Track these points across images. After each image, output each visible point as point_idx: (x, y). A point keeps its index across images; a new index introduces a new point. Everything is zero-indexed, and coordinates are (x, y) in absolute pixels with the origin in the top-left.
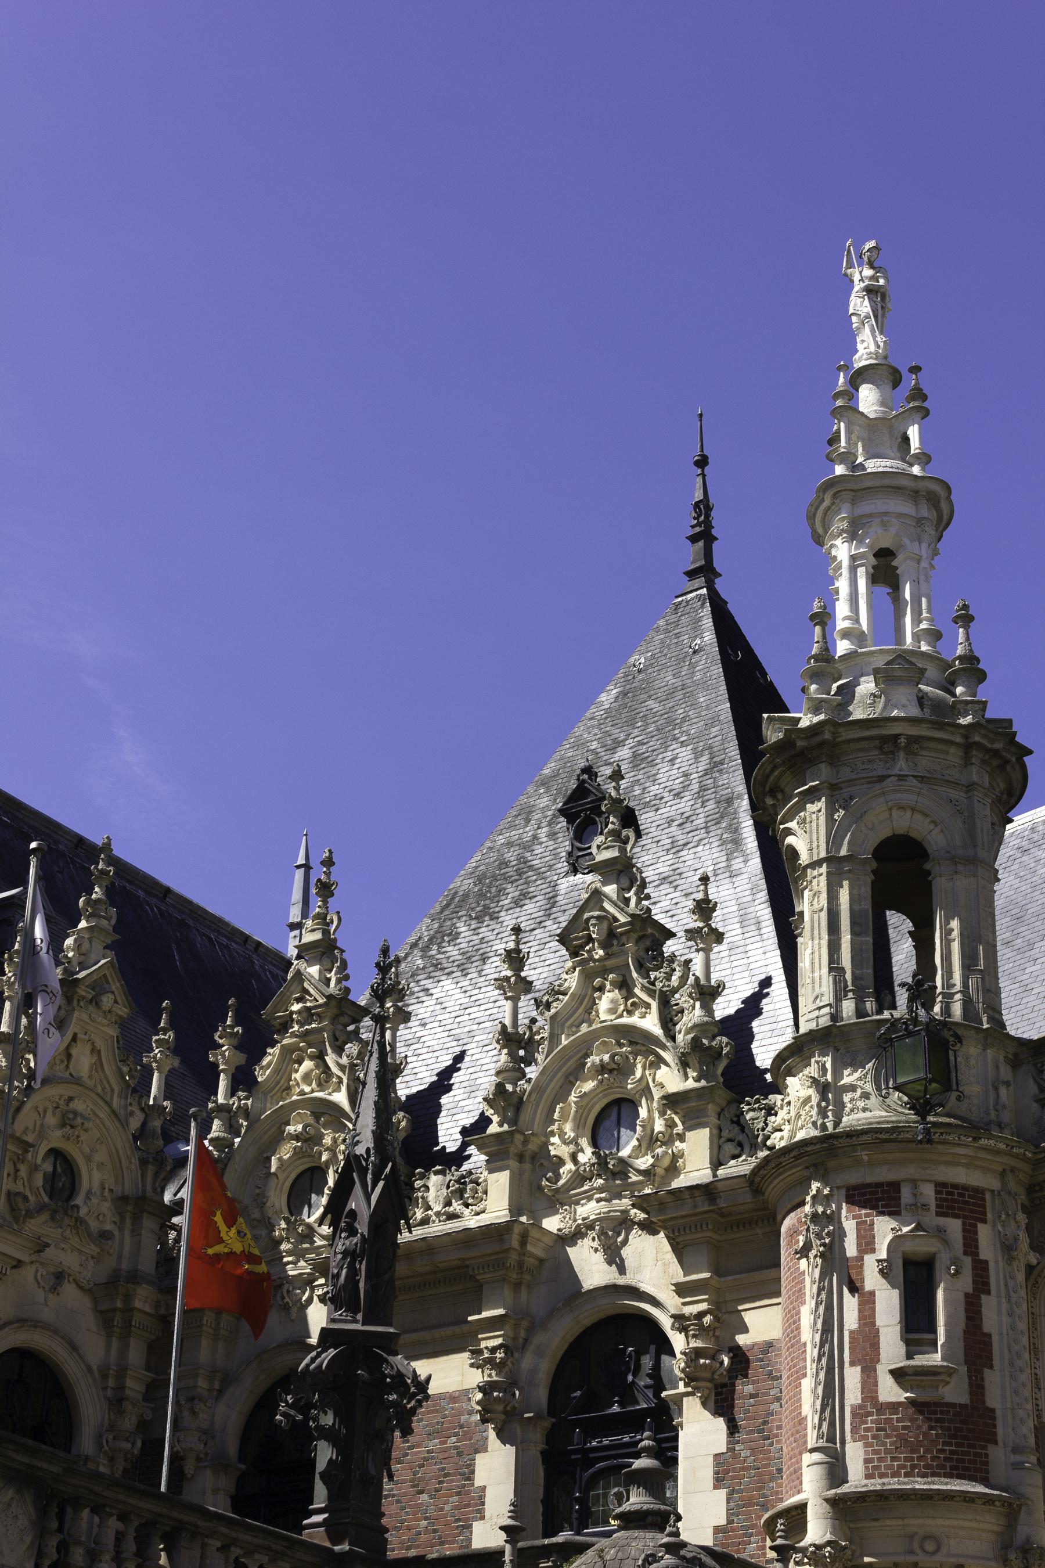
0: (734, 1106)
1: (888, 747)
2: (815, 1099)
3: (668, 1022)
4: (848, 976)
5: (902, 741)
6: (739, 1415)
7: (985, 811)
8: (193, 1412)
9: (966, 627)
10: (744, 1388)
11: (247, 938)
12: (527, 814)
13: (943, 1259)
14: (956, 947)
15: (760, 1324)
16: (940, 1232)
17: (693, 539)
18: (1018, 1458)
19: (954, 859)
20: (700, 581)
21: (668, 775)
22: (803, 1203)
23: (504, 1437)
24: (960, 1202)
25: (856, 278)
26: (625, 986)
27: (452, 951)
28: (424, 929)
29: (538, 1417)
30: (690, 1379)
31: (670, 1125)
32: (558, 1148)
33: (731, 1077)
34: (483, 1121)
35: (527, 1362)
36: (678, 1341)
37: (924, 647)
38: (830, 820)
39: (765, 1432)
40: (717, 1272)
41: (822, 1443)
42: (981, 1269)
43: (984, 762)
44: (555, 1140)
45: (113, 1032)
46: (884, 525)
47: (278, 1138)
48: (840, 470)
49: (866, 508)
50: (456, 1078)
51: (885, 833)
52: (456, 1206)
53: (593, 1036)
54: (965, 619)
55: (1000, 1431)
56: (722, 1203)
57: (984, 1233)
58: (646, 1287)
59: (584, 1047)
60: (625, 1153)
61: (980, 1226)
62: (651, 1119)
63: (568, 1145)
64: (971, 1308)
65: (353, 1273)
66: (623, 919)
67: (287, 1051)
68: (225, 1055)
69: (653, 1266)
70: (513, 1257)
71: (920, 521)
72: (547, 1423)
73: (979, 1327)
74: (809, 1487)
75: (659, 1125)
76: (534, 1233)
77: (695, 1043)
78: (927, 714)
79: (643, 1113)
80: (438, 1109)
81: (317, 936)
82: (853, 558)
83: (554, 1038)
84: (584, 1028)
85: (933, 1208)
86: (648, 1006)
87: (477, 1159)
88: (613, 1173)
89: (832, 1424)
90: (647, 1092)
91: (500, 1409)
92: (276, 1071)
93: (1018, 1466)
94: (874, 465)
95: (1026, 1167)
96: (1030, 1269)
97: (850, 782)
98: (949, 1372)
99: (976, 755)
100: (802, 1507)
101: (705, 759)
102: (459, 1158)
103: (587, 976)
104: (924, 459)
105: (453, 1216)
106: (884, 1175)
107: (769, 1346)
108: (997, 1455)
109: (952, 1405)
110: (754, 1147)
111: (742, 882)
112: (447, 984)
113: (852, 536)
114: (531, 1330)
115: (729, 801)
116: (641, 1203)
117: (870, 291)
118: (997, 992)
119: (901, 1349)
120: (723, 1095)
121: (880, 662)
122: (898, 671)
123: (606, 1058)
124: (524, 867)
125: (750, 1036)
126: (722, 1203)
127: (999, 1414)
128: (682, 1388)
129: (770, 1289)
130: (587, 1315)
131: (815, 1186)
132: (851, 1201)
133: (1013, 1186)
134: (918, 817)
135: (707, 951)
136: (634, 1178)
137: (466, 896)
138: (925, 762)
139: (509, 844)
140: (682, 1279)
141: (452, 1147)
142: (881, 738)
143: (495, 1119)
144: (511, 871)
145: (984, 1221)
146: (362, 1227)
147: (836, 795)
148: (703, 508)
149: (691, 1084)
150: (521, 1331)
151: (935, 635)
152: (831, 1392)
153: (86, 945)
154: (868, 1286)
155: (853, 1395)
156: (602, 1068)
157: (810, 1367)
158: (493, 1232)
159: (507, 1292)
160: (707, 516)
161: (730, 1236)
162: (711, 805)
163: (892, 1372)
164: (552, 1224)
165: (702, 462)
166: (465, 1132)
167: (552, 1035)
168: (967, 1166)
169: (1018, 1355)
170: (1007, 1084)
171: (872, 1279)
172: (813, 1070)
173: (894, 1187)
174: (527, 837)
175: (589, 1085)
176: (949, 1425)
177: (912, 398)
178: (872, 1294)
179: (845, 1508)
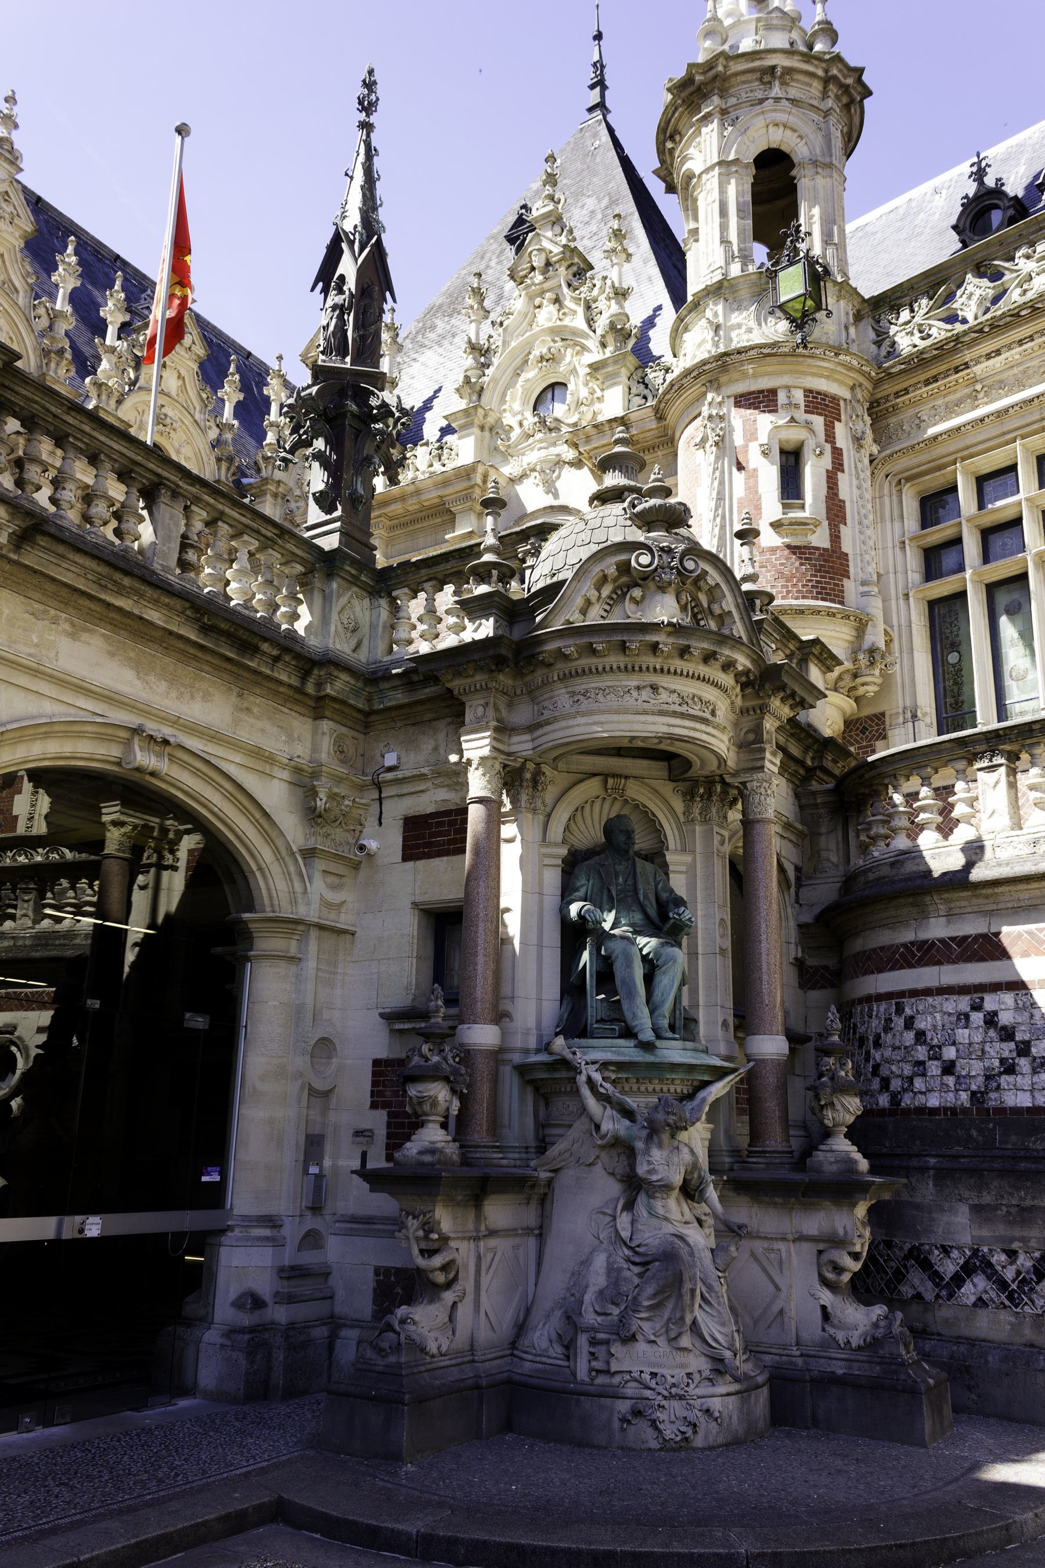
0: (639, 373)
1: (767, 78)
3: (590, 322)
4: (735, 248)
16: (808, 424)
17: (592, 87)
18: (866, 589)
19: (815, 163)
24: (820, 404)
26: (557, 301)
27: (432, 336)
32: (508, 419)
42: (837, 453)
44: (507, 415)
45: (195, 367)
50: (435, 402)
51: (764, 147)
55: (852, 570)
61: (836, 423)
62: (577, 390)
63: (515, 412)
73: (837, 495)
75: (584, 393)
80: (424, 420)
85: (803, 407)
86: (575, 312)
90: (574, 371)
93: (864, 594)
98: (817, 524)
99: (833, 88)
103: (531, 298)
106: (764, 383)
108: (850, 587)
109: (817, 549)
112: (429, 353)
120: (632, 361)
123: (545, 351)
126: (634, 431)
127: (851, 558)
131: (710, 396)
132: (738, 404)
134: (788, 132)
137: (441, 306)
145: (839, 420)
146: (351, 284)
148: (599, 66)
158: (466, 473)
159: (473, 517)
163: (772, 525)
165: (598, 37)
167: (504, 342)
168: (827, 377)
169: (865, 517)
171: (754, 459)
173: (773, 392)
178: (755, 470)
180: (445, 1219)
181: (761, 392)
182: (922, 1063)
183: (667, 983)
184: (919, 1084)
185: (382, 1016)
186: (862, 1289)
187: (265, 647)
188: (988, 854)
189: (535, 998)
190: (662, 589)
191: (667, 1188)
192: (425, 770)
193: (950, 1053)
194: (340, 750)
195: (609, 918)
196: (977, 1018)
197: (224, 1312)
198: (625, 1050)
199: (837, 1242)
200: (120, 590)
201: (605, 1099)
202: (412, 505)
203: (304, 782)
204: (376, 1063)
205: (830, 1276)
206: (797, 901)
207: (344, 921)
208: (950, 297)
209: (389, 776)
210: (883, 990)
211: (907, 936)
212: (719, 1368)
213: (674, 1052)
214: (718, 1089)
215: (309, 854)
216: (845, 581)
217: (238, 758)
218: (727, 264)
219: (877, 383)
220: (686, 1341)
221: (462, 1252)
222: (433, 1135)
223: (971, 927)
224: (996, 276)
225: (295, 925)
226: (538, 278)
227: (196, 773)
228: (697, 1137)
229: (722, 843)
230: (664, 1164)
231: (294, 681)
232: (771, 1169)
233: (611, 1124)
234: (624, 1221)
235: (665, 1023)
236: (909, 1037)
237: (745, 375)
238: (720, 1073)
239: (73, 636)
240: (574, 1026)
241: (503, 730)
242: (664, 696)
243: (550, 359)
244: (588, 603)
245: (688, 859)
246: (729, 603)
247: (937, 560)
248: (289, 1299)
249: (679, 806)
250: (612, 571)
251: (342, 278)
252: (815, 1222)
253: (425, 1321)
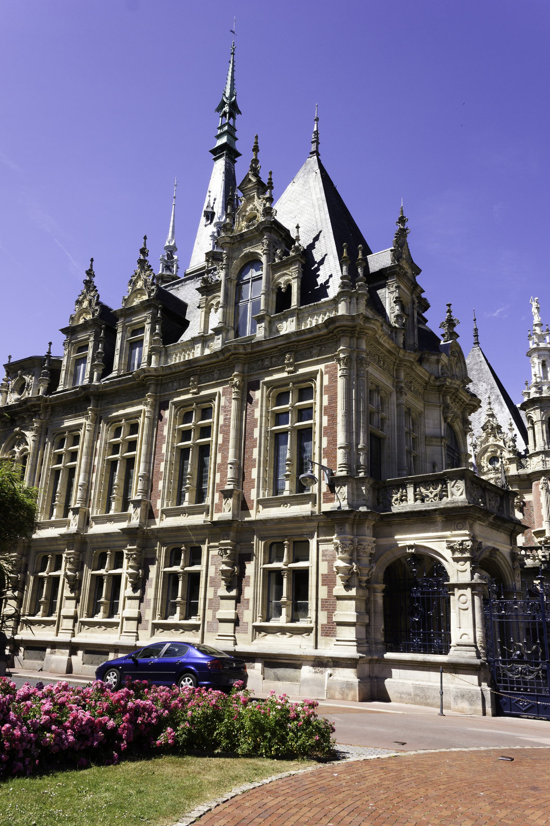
17: (475, 336)
26: (495, 437)
39: (530, 515)
49: (541, 353)
53: (490, 445)
59: (488, 447)
83: (481, 445)
103: (487, 434)
107: (530, 502)
111: (505, 414)
113: (538, 358)
115: (498, 396)
148: (476, 330)
156: (492, 451)
175: (489, 454)
226: (490, 431)
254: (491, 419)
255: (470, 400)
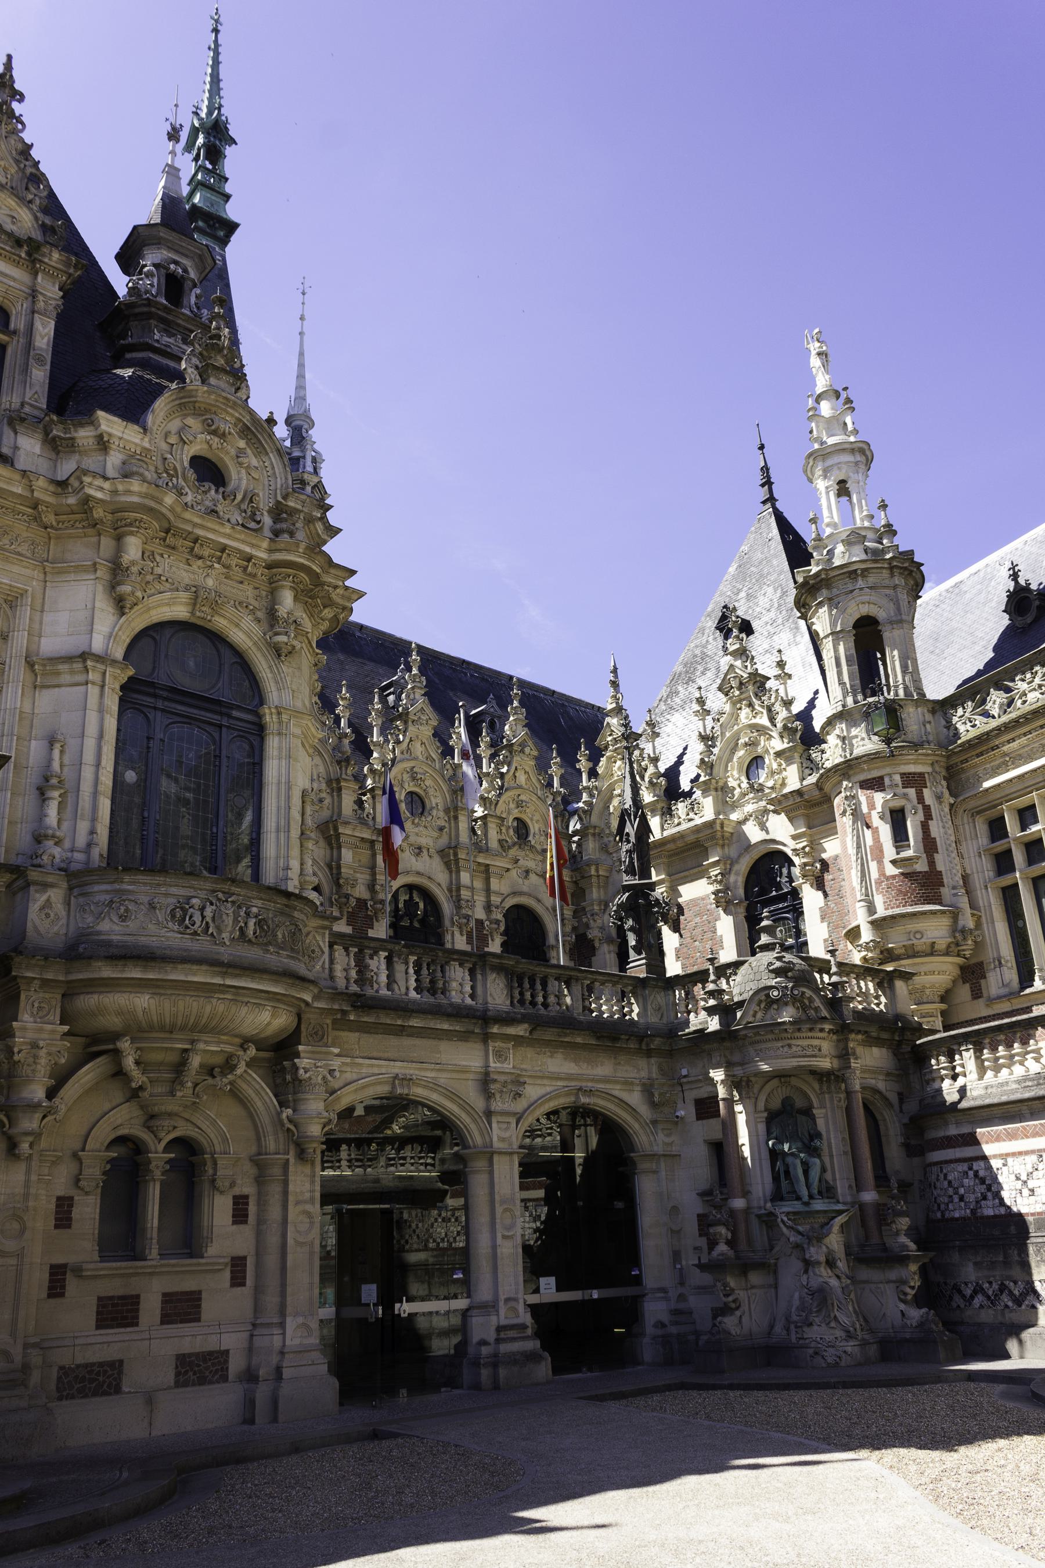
0: (806, 753)
2: (840, 744)
3: (772, 720)
4: (848, 686)
5: (859, 572)
6: (827, 889)
7: (903, 597)
8: (595, 921)
9: (885, 510)
10: (827, 877)
11: (593, 706)
12: (702, 630)
13: (908, 808)
14: (897, 664)
15: (831, 848)
16: (905, 796)
17: (763, 485)
18: (955, 891)
20: (769, 505)
21: (763, 601)
22: (840, 792)
23: (726, 911)
25: (812, 349)
26: (751, 705)
27: (677, 700)
28: (664, 692)
29: (741, 902)
30: (804, 876)
31: (780, 765)
32: (732, 783)
33: (806, 737)
34: (698, 776)
35: (732, 878)
36: (797, 860)
37: (866, 524)
38: (830, 615)
39: (840, 895)
40: (809, 827)
41: (863, 897)
42: (927, 809)
43: (900, 573)
45: (533, 763)
46: (839, 468)
47: (611, 797)
48: (816, 446)
49: (829, 462)
50: (685, 758)
52: (692, 815)
54: (884, 506)
55: (945, 881)
56: (806, 797)
57: (927, 793)
58: (778, 839)
59: (736, 737)
60: (761, 781)
62: (771, 763)
63: (736, 779)
64: (925, 827)
65: (631, 859)
66: (745, 675)
67: (609, 758)
68: (583, 765)
69: (781, 830)
70: (719, 834)
71: (856, 463)
72: (745, 904)
74: (860, 918)
75: (775, 766)
76: (726, 822)
77: (785, 727)
78: (870, 557)
79: (767, 761)
80: (679, 773)
81: (614, 705)
82: (827, 488)
83: (723, 734)
84: (736, 727)
87: (698, 794)
88: (757, 790)
89: (866, 888)
90: (767, 751)
91: (724, 901)
92: (606, 768)
93: (955, 895)
94: (831, 441)
95: (944, 759)
96: (952, 806)
97: (837, 596)
98: (918, 858)
99: (896, 571)
100: (858, 927)
101: (779, 591)
102: (690, 794)
103: (734, 704)
104: (856, 432)
105: (690, 820)
106: (875, 774)
108: (945, 892)
109: (920, 872)
110: (818, 769)
113: (825, 477)
114: (732, 865)
116: (771, 802)
117: (819, 354)
118: (920, 681)
119: (894, 850)
120: (801, 748)
121: (844, 536)
122: (855, 538)
123: (747, 739)
124: (704, 656)
125: (812, 718)
126: (806, 797)
127: (944, 873)
128: (801, 881)
129: (834, 832)
130: (755, 855)
131: (845, 783)
132: (862, 787)
133: (937, 769)
134: (872, 606)
135: (785, 684)
136: (767, 791)
137: (680, 674)
138: (872, 579)
139: (697, 646)
140: (794, 833)
141: (687, 789)
142: (850, 573)
143: (703, 774)
144: (699, 659)
146: (633, 839)
147: (831, 602)
148: (765, 469)
149: (786, 746)
150: (728, 865)
151: (871, 517)
152: (864, 874)
153: (514, 728)
154: (875, 825)
155: (874, 874)
156: (746, 744)
157: (854, 865)
158: (710, 825)
159: (719, 849)
160: (768, 473)
161: (813, 809)
162: (784, 612)
164: (734, 816)
165: (762, 447)
166: (692, 781)
169: (950, 845)
170: (930, 722)
171: (876, 821)
172: (837, 731)
173: (881, 778)
174: (704, 642)
176: (924, 883)
177: (846, 403)
179: (878, 925)
180: (732, 1282)
181: (874, 779)
182: (951, 1197)
183: (815, 1173)
184: (951, 1207)
185: (698, 1194)
186: (918, 1301)
187: (623, 1037)
188: (968, 1093)
189: (761, 1185)
190: (786, 1004)
191: (819, 1263)
192: (700, 1077)
193: (962, 1191)
194: (661, 1069)
195: (786, 1147)
196: (971, 1173)
197: (649, 1330)
198: (797, 1206)
199: (903, 1282)
200: (566, 1035)
201: (788, 1227)
202: (680, 844)
203: (648, 1090)
204: (698, 1215)
205: (902, 1297)
206: (901, 1111)
207: (675, 1149)
208: (984, 702)
209: (685, 1080)
210: (935, 1160)
211: (941, 1134)
212: (849, 1336)
213: (819, 1205)
214: (840, 1220)
215: (654, 1122)
216: (942, 889)
217: (618, 1087)
218: (845, 697)
219: (948, 757)
220: (833, 1324)
221: (742, 1295)
222: (722, 1248)
223: (965, 1130)
224: (1008, 690)
225: (653, 1156)
226: (737, 693)
227: (603, 1098)
228: (835, 1241)
229: (840, 1101)
230: (817, 1254)
231: (637, 1046)
232: (870, 1253)
233: (794, 1238)
234: (804, 1279)
235: (816, 1191)
236: (946, 1183)
237: (863, 770)
238: (840, 1212)
239: (551, 1057)
240: (777, 1196)
241: (728, 1066)
242: (794, 1048)
243: (752, 744)
244: (756, 1012)
245: (824, 1111)
246: (818, 1003)
247: (1003, 863)
248: (677, 1323)
249: (816, 1086)
250: (763, 998)
251: (628, 834)
252: (893, 1274)
253: (729, 1322)
254: (738, 663)
255: (270, 551)
